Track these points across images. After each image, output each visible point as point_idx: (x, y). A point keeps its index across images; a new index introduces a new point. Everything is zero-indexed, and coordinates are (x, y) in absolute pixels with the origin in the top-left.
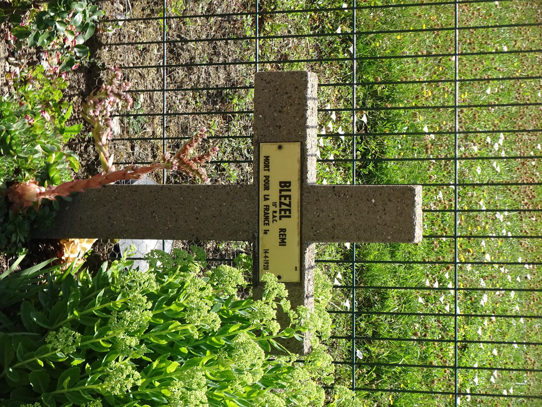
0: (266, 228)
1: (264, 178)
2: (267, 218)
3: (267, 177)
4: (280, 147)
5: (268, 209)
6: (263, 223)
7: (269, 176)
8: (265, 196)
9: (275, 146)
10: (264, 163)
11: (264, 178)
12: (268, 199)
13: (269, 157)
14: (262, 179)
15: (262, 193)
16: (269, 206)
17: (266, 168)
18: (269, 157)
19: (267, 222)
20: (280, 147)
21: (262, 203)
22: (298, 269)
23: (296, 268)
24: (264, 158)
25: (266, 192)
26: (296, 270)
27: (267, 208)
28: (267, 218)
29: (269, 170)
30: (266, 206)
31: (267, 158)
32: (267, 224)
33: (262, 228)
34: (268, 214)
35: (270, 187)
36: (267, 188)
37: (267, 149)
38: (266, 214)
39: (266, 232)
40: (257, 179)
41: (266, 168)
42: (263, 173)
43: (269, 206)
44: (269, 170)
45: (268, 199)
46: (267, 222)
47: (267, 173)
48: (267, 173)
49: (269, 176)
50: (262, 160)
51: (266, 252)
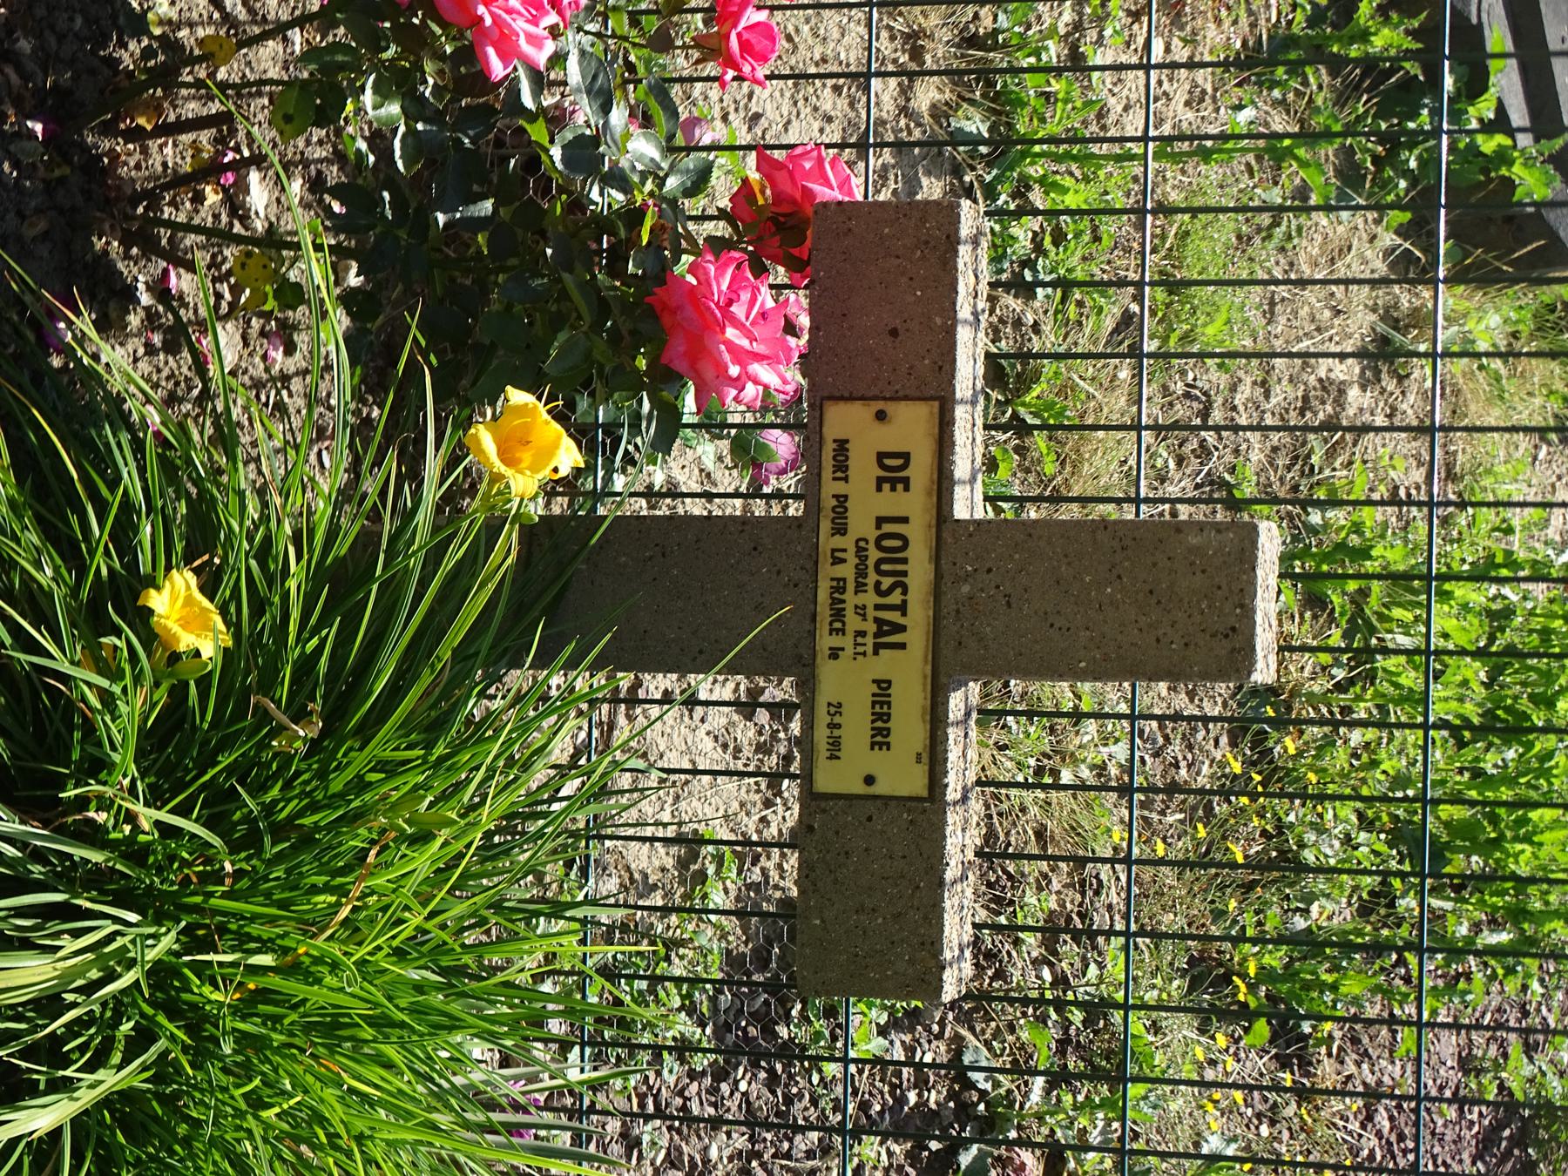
0: (836, 641)
1: (834, 502)
3: (842, 499)
4: (881, 416)
5: (843, 590)
7: (846, 497)
8: (834, 551)
10: (834, 458)
11: (834, 502)
12: (844, 561)
13: (847, 441)
15: (827, 541)
16: (844, 580)
17: (839, 474)
18: (847, 441)
19: (838, 625)
21: (827, 572)
22: (925, 758)
23: (919, 755)
24: (835, 446)
25: (838, 542)
26: (919, 760)
28: (838, 615)
29: (846, 479)
30: (838, 580)
31: (842, 446)
32: (837, 631)
33: (825, 641)
34: (843, 601)
36: (841, 530)
37: (844, 420)
38: (835, 601)
39: (834, 654)
40: (813, 509)
41: (839, 474)
42: (830, 488)
43: (844, 580)
44: (846, 479)
45: (844, 561)
46: (838, 625)
47: (840, 487)
48: (840, 487)
49: (846, 497)
50: (829, 447)
51: (836, 708)
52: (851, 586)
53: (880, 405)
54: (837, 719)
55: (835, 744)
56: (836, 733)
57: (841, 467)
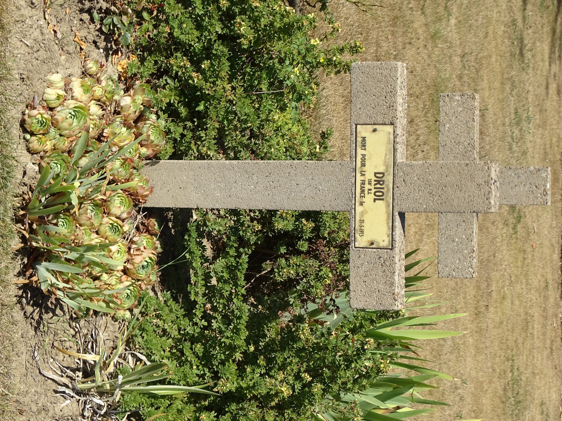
2: (363, 191)
3: (364, 156)
6: (359, 196)
12: (365, 175)
14: (359, 157)
17: (363, 148)
20: (375, 130)
21: (359, 178)
28: (363, 191)
29: (365, 149)
31: (364, 139)
38: (362, 188)
42: (360, 152)
44: (365, 149)
47: (363, 152)
48: (363, 152)
50: (359, 139)
52: (367, 182)
54: (363, 224)
55: (362, 231)
56: (362, 228)
57: (364, 146)
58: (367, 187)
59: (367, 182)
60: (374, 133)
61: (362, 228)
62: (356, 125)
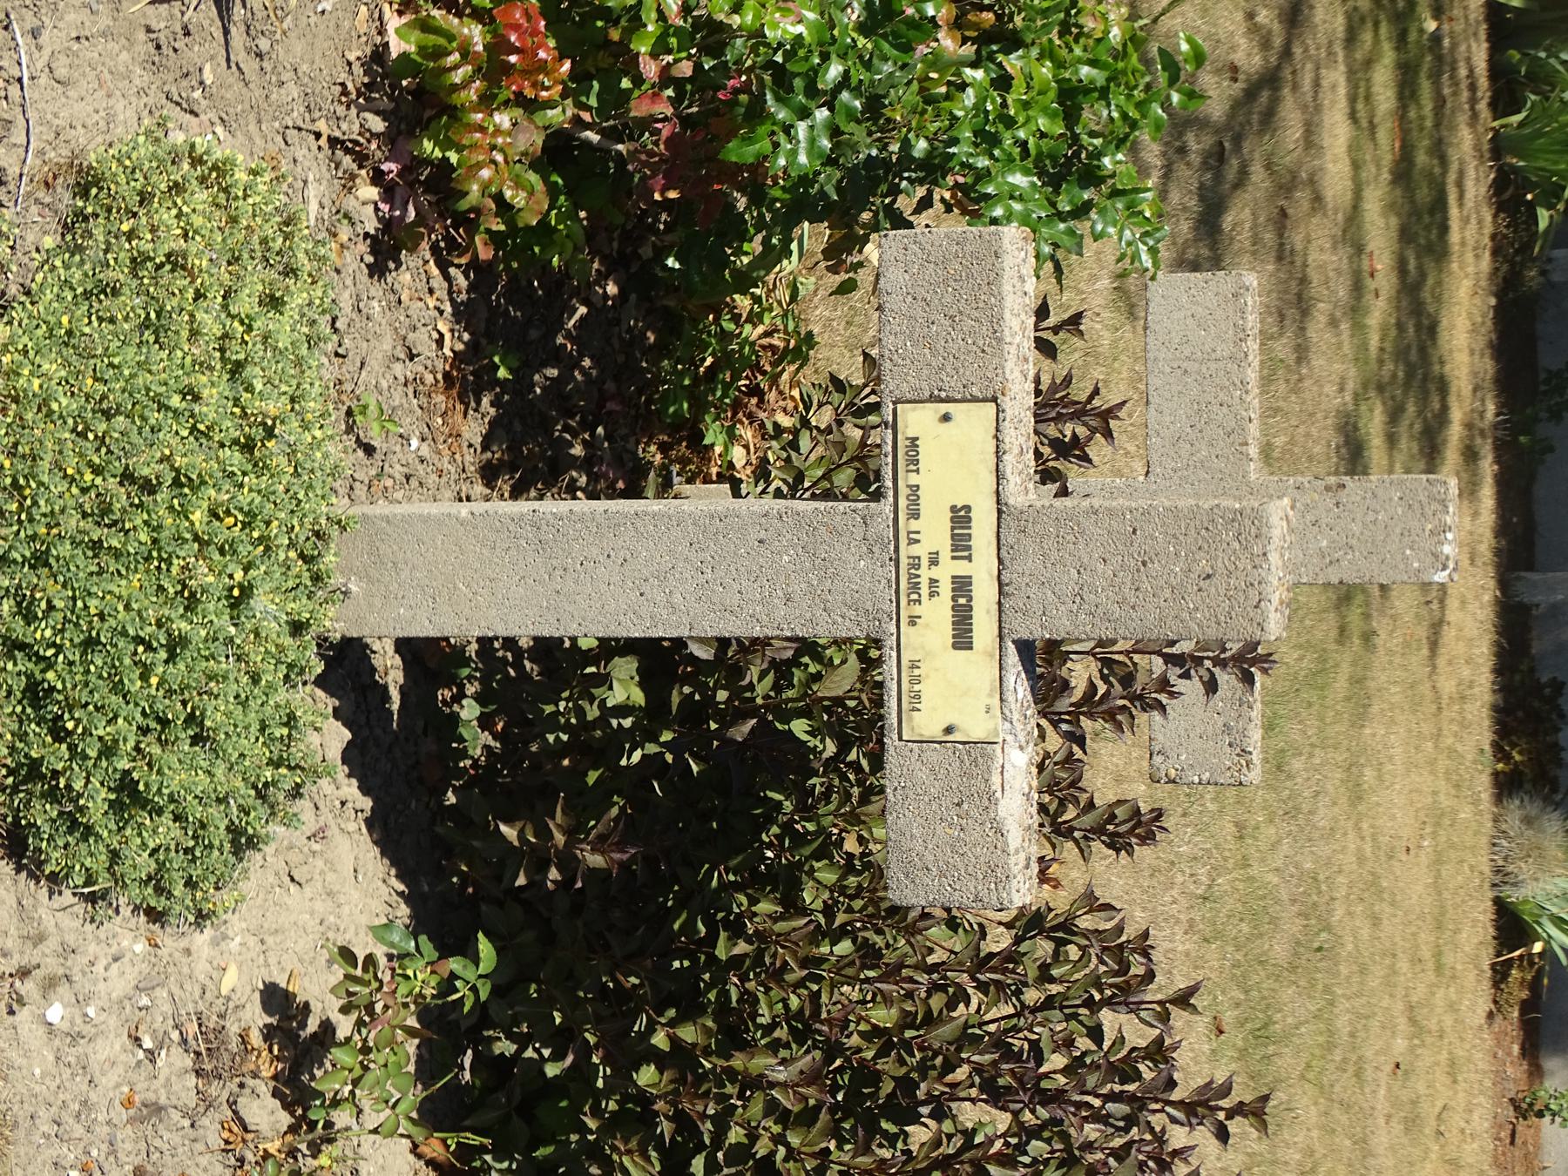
0: (917, 609)
3: (915, 489)
5: (918, 567)
9: (932, 411)
14: (903, 491)
17: (912, 467)
19: (914, 597)
20: (946, 418)
27: (915, 563)
28: (915, 587)
29: (917, 471)
35: (922, 512)
36: (915, 515)
38: (911, 576)
39: (913, 621)
44: (917, 471)
47: (914, 479)
48: (914, 479)
52: (925, 562)
53: (944, 408)
55: (917, 696)
56: (916, 688)
57: (914, 461)
58: (925, 574)
59: (925, 562)
60: (946, 425)
61: (916, 688)
62: (894, 403)
